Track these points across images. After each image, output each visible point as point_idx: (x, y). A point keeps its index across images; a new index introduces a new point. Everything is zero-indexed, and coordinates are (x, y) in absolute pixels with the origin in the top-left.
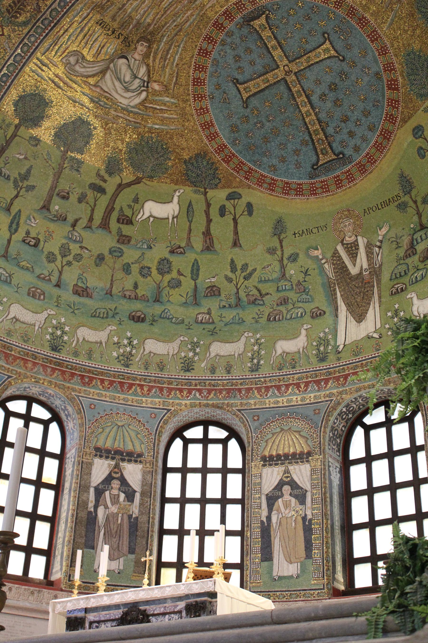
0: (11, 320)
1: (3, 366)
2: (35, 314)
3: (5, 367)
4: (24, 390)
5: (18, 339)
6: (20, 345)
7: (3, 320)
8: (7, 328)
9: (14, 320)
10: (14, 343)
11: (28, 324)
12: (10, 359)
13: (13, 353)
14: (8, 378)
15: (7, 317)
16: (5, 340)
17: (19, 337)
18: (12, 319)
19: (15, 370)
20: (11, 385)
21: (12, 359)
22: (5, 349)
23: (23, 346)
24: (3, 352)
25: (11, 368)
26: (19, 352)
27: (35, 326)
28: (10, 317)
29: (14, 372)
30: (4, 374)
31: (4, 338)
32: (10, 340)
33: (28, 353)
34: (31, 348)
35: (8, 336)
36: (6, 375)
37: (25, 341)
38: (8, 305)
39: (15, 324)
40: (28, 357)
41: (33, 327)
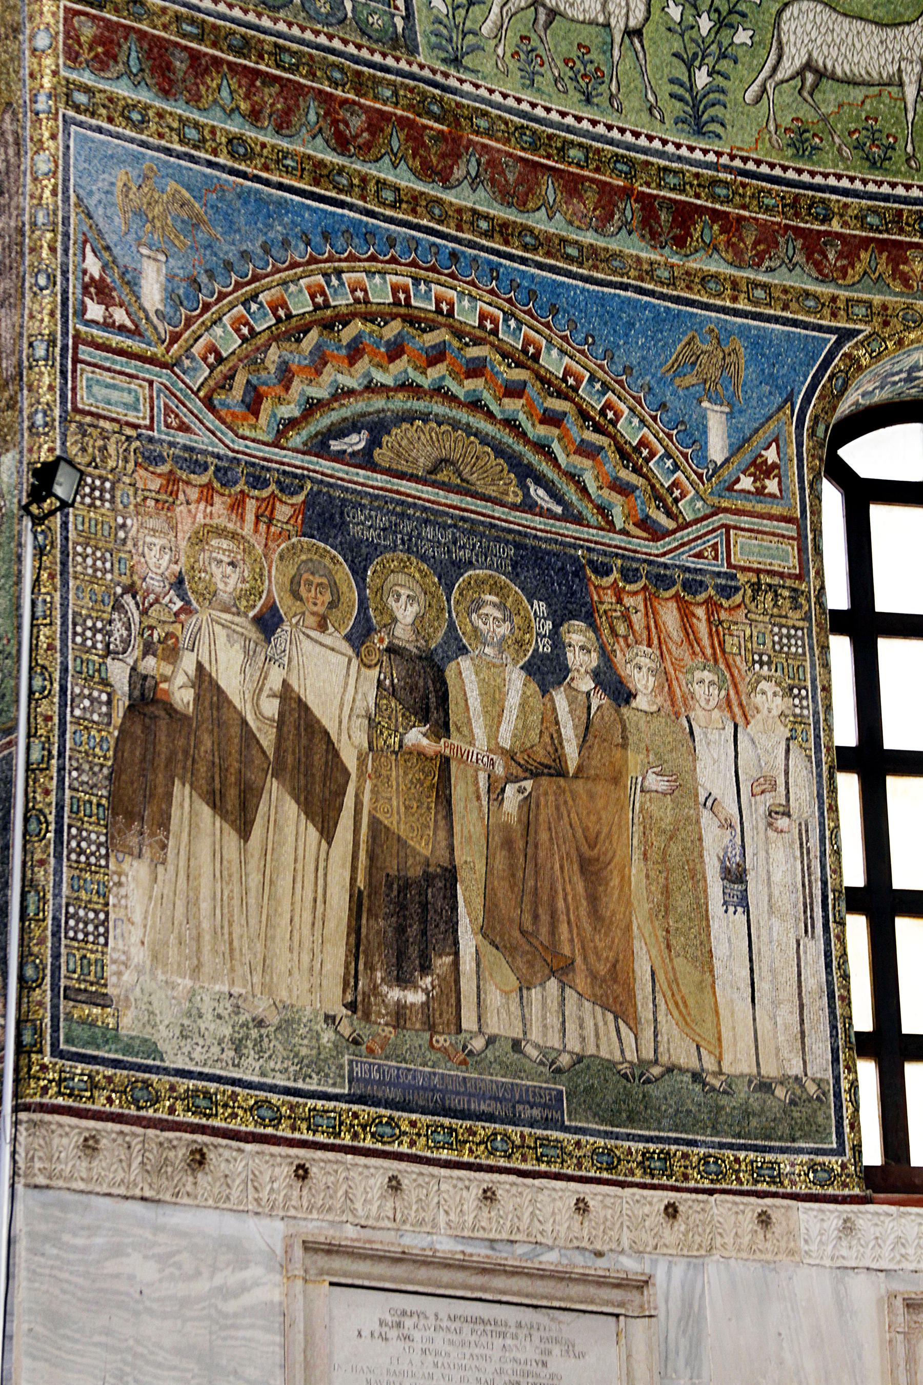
0: (797, 82)
1: (807, 294)
2: (891, 33)
3: (816, 298)
4: (910, 379)
5: (844, 159)
6: (858, 185)
7: (764, 90)
8: (786, 122)
9: (810, 77)
10: (832, 181)
11: (864, 83)
12: (831, 256)
13: (836, 226)
14: (838, 344)
15: (775, 69)
16: (791, 175)
17: (846, 151)
18: (800, 73)
19: (859, 301)
20: (860, 368)
21: (840, 255)
22: (797, 215)
23: (872, 188)
24: (796, 229)
25: (843, 294)
26: (861, 219)
27: (901, 84)
28: (788, 68)
29: (861, 311)
30: (820, 328)
31: (785, 169)
32: (813, 174)
33: (900, 213)
34: (908, 187)
35: (797, 156)
36: (829, 330)
37: (873, 165)
38: (769, 18)
39: (818, 96)
40: (901, 231)
41: (894, 90)
